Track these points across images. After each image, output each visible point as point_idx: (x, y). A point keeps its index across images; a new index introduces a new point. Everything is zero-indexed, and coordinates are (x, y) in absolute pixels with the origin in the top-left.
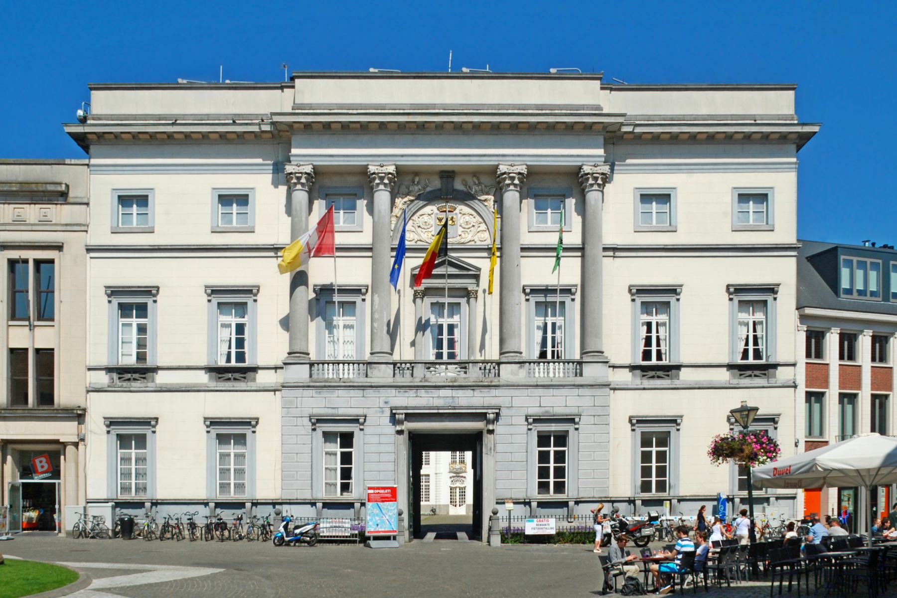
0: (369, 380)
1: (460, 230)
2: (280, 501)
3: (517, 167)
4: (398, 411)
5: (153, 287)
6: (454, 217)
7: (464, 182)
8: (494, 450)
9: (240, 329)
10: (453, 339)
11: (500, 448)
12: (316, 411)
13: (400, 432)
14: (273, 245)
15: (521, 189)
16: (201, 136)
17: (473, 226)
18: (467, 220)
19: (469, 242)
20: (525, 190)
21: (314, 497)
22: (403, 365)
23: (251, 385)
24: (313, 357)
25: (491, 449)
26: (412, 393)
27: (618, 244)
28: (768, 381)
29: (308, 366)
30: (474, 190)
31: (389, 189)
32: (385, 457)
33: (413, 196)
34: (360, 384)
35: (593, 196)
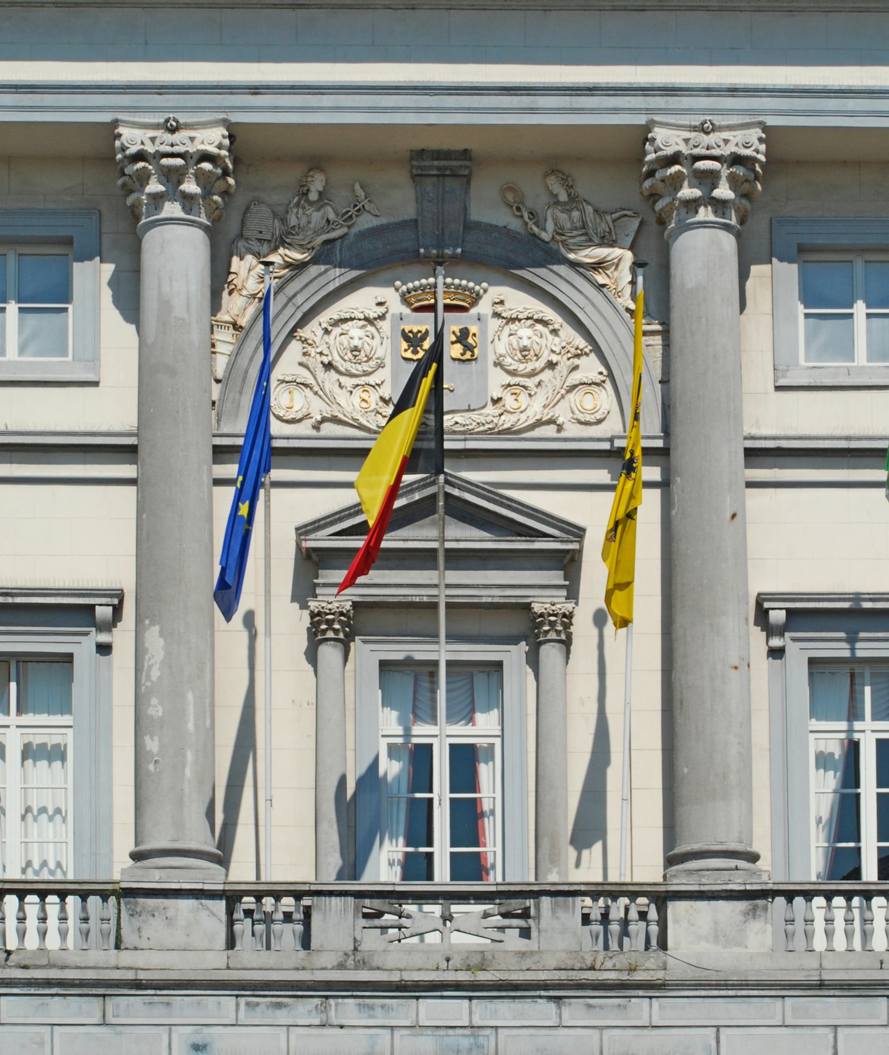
0: (126, 958)
1: (496, 380)
3: (725, 135)
6: (473, 329)
7: (510, 197)
15: (742, 222)
17: (551, 365)
18: (525, 342)
30: (550, 226)
33: (302, 248)
34: (90, 975)
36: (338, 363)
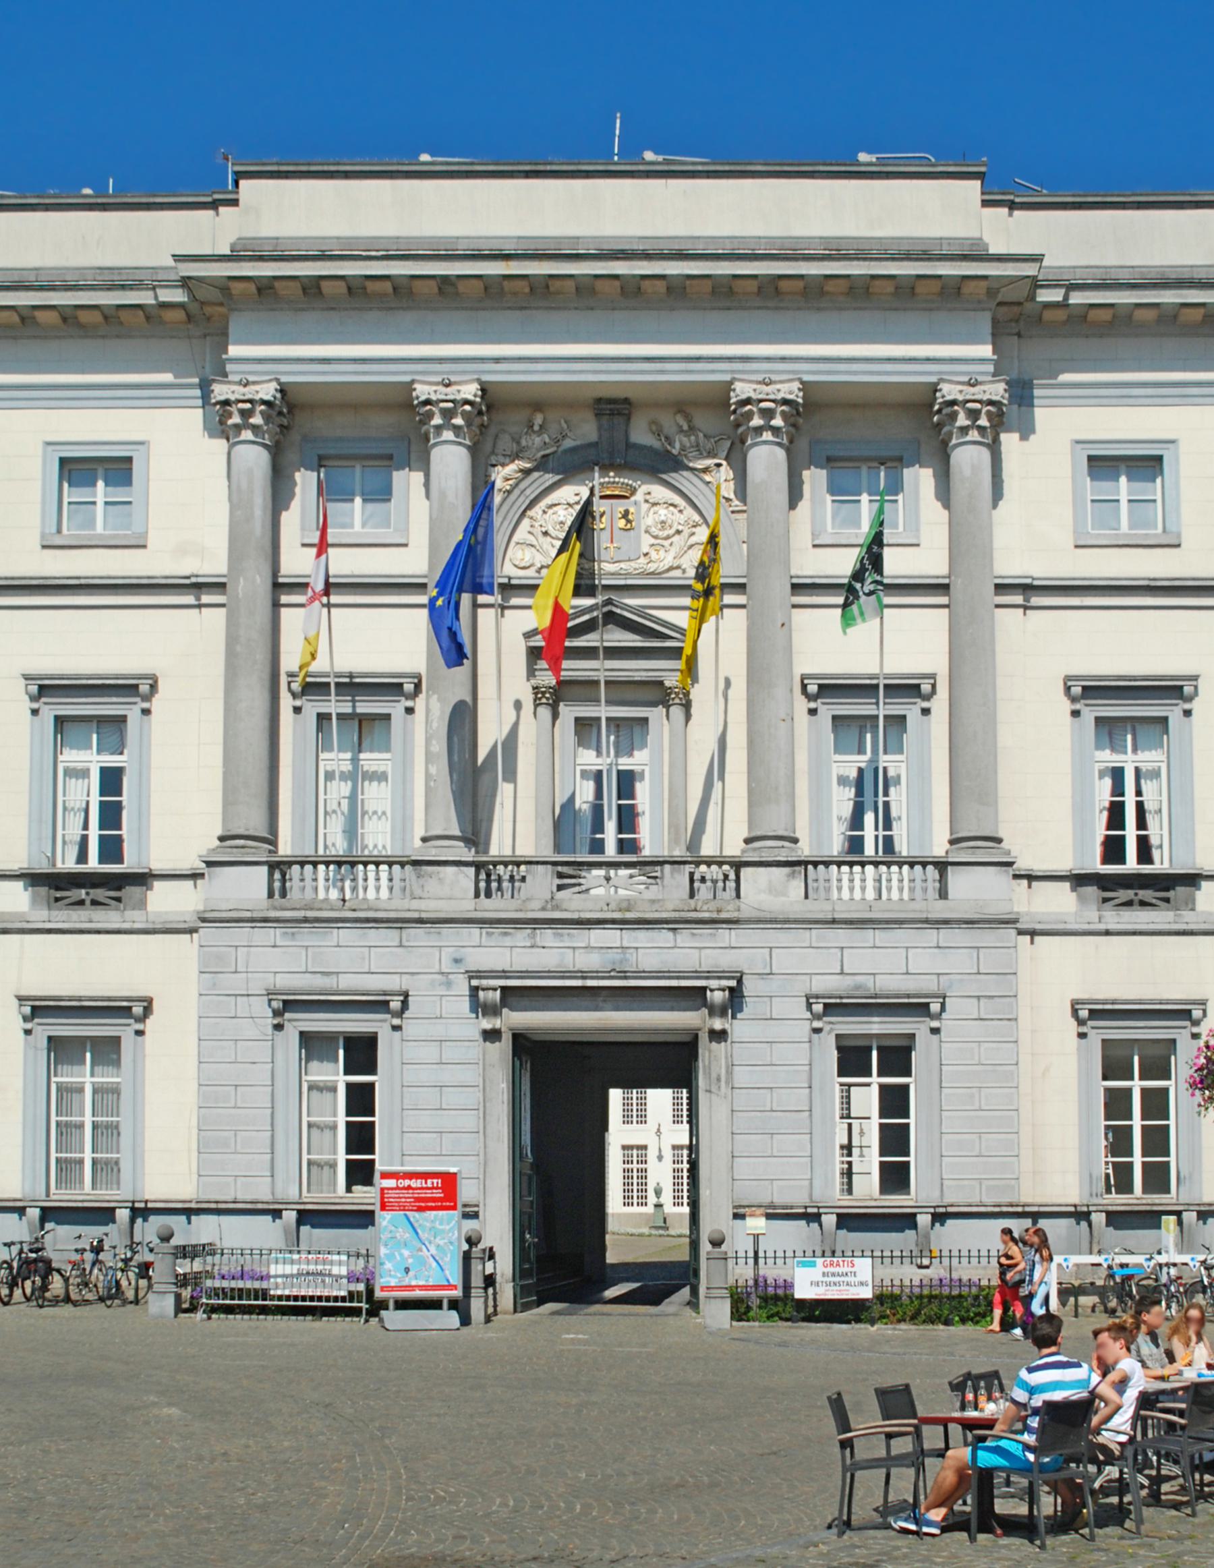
0: (415, 904)
1: (647, 541)
4: (485, 983)
6: (632, 510)
7: (654, 428)
8: (727, 1083)
9: (111, 780)
10: (633, 807)
11: (742, 1076)
12: (283, 982)
15: (791, 442)
17: (678, 532)
20: (803, 444)
22: (500, 868)
25: (719, 1080)
26: (521, 937)
27: (1035, 575)
29: (265, 869)
30: (677, 445)
31: (468, 442)
32: (452, 1098)
33: (530, 460)
34: (392, 915)
36: (552, 531)
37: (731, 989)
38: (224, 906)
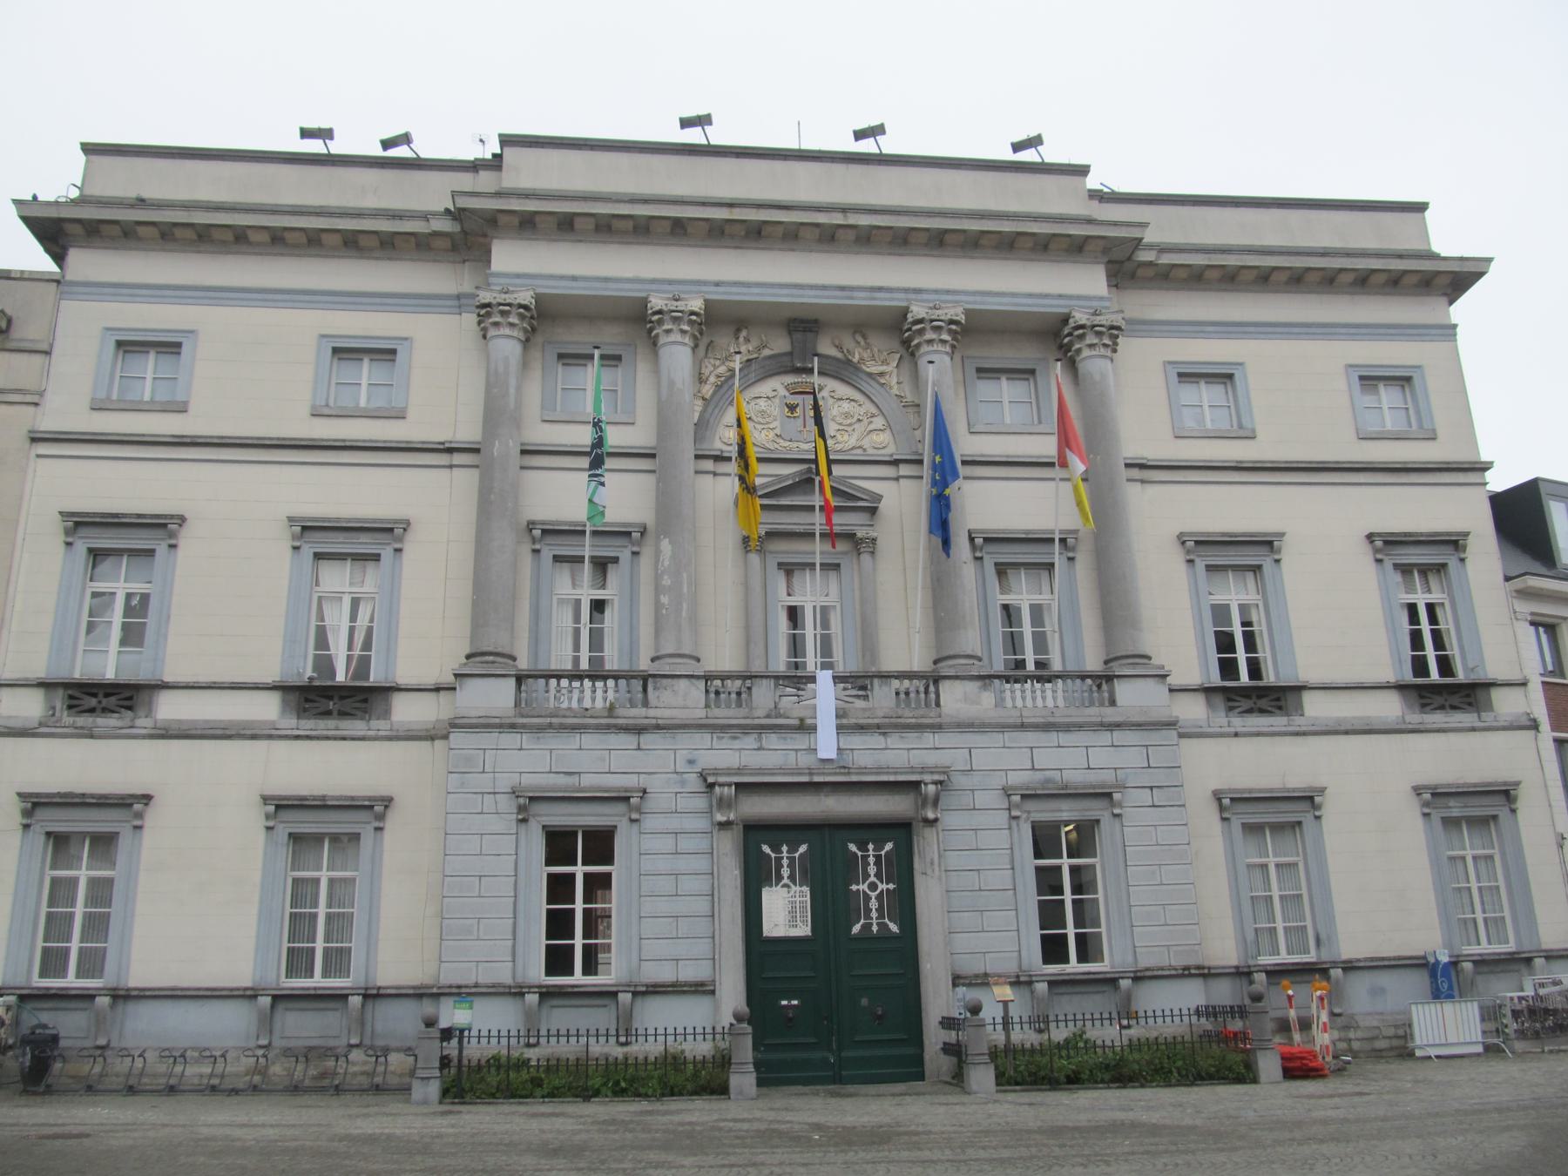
0: (652, 713)
2: (435, 990)
4: (722, 779)
5: (172, 517)
12: (527, 780)
13: (724, 825)
14: (443, 443)
16: (304, 240)
19: (852, 449)
21: (520, 980)
23: (379, 725)
24: (523, 664)
25: (932, 863)
26: (750, 741)
28: (1479, 717)
29: (512, 681)
30: (857, 356)
35: (1093, 363)
36: (754, 418)
37: (941, 782)
38: (474, 713)
